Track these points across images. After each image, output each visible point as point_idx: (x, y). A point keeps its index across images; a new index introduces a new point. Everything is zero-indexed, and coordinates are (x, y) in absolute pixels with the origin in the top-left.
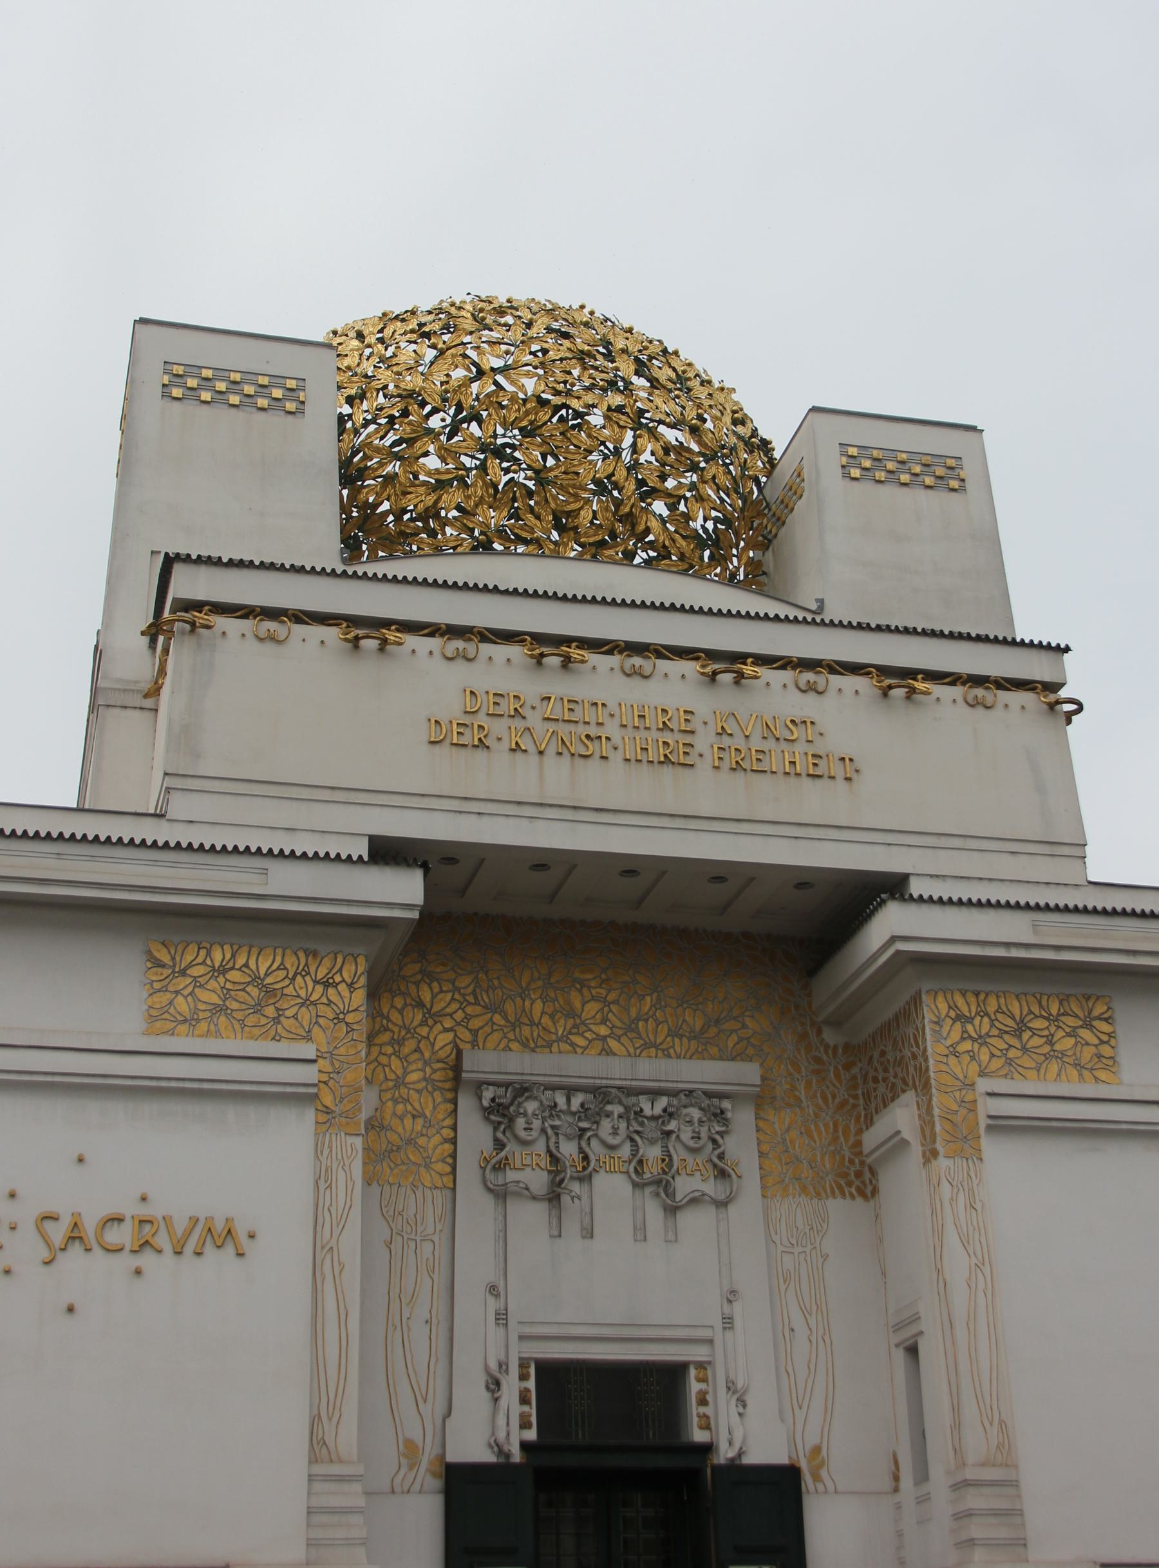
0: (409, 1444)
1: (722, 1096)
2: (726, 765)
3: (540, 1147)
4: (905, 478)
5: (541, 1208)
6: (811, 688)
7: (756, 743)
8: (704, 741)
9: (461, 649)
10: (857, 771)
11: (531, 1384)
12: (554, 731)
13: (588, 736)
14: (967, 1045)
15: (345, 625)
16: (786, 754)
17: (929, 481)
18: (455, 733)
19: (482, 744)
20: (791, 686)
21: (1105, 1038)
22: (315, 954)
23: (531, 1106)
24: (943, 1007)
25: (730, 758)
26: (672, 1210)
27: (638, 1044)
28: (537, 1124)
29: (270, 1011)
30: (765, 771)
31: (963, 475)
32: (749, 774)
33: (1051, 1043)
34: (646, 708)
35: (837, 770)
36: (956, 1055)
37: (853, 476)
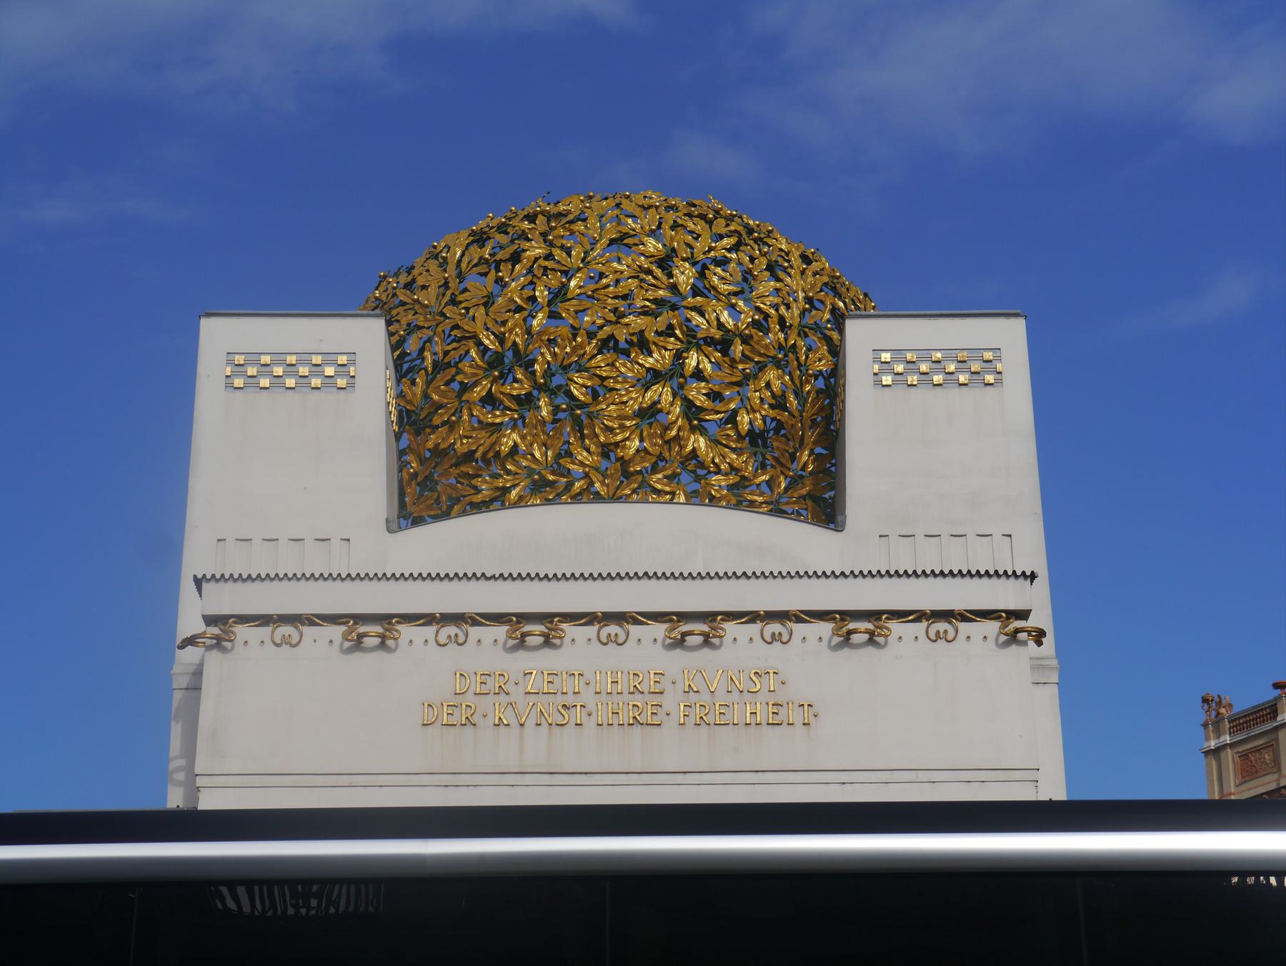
2: (691, 721)
4: (937, 378)
6: (775, 638)
7: (721, 698)
8: (672, 701)
9: (453, 636)
10: (815, 716)
12: (534, 704)
13: (564, 706)
15: (352, 622)
16: (748, 705)
17: (962, 379)
18: (445, 714)
19: (469, 722)
20: (757, 638)
30: (728, 724)
31: (999, 367)
32: (712, 726)
34: (619, 674)
35: (796, 716)
37: (884, 383)
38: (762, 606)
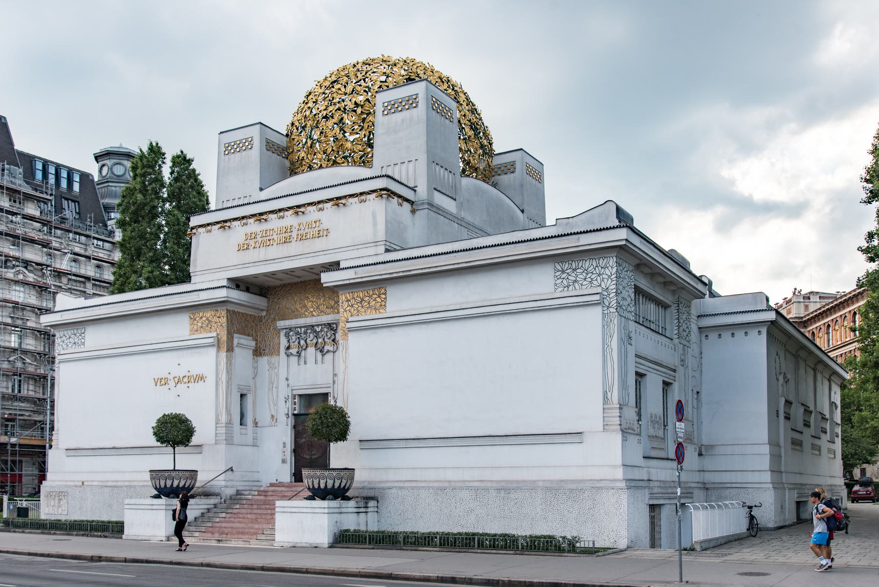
0: (272, 416)
1: (333, 324)
3: (296, 343)
5: (297, 357)
6: (321, 209)
7: (306, 230)
8: (294, 234)
11: (296, 400)
14: (349, 308)
20: (316, 210)
21: (383, 300)
22: (217, 310)
23: (291, 333)
24: (344, 298)
25: (299, 237)
26: (323, 355)
27: (319, 311)
28: (293, 337)
29: (210, 326)
33: (369, 304)
36: (346, 311)
38: (316, 200)
